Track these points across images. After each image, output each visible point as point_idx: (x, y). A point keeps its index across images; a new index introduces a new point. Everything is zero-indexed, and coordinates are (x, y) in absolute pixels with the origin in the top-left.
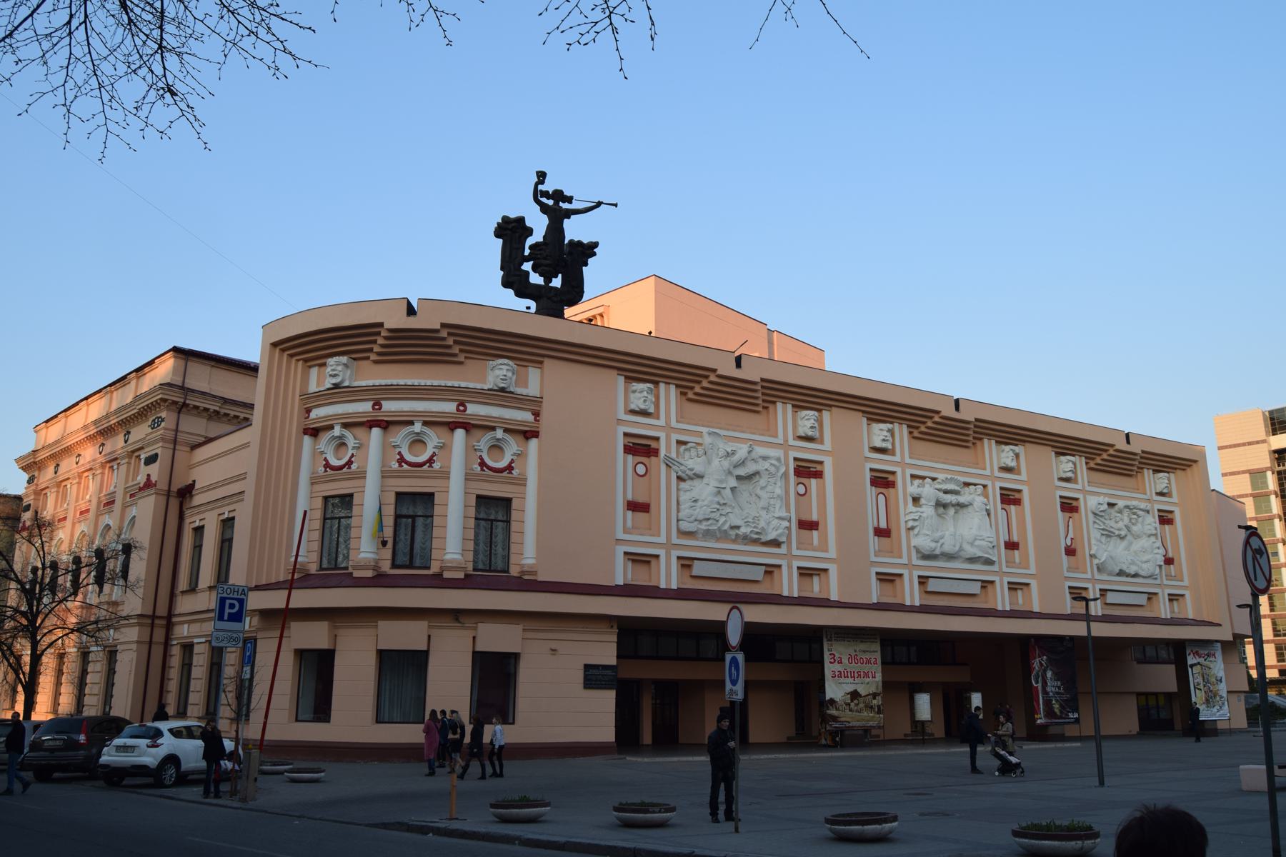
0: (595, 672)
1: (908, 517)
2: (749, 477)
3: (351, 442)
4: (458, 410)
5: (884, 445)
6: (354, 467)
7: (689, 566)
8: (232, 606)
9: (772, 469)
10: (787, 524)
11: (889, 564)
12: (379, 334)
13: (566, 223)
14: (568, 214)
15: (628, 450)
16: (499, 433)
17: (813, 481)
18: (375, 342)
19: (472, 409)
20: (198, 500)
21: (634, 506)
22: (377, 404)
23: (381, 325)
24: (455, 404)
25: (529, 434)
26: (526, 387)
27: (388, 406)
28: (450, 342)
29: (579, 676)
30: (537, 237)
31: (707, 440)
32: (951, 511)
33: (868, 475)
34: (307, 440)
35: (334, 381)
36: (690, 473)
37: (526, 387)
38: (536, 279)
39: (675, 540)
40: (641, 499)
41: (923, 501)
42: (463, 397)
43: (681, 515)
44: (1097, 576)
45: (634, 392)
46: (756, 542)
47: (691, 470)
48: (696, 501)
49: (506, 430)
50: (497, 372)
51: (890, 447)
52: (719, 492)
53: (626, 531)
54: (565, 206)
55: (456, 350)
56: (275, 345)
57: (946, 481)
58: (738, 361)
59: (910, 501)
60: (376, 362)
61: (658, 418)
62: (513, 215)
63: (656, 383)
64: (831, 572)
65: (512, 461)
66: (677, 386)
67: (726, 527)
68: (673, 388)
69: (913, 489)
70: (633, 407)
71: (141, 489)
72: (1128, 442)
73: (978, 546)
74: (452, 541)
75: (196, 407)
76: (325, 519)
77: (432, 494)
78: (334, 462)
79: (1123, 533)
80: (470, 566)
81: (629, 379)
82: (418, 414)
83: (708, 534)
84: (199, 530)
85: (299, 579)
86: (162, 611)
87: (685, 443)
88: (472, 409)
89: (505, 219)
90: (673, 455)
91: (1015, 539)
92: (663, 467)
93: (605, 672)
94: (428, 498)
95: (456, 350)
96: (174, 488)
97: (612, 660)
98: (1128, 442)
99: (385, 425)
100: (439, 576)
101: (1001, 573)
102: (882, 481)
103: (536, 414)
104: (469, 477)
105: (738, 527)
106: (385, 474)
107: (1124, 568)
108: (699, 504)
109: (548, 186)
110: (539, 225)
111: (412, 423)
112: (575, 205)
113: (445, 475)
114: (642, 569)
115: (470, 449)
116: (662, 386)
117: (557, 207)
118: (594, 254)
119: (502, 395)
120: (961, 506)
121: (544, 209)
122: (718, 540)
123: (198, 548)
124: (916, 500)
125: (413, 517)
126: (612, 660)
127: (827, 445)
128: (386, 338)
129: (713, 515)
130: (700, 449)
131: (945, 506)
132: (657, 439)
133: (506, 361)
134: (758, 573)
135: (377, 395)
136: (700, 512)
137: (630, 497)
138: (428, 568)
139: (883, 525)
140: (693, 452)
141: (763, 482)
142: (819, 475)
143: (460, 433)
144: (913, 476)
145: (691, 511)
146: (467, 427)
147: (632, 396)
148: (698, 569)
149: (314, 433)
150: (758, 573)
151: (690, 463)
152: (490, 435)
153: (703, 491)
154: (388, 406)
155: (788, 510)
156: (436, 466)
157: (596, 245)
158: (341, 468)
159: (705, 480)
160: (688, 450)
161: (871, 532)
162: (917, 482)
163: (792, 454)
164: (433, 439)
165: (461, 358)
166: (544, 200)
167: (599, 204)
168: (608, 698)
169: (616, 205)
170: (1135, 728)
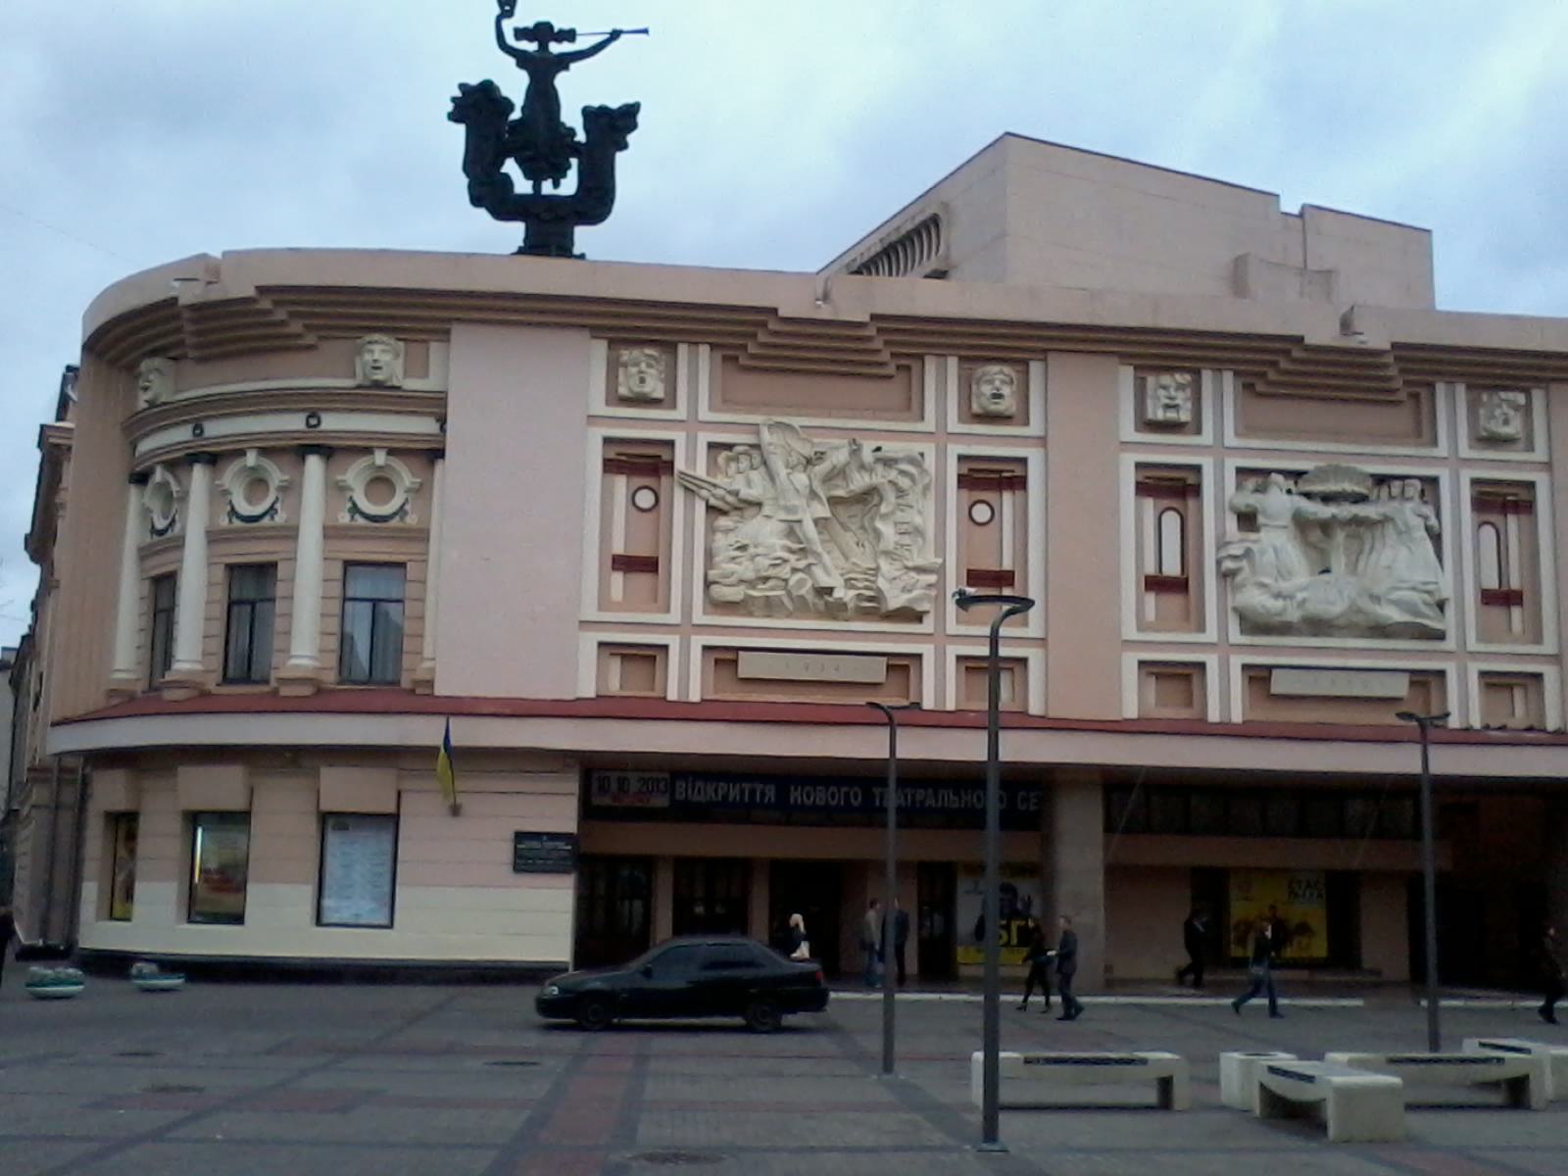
0: (535, 844)
1: (1223, 553)
2: (867, 497)
3: (174, 487)
4: (308, 424)
5: (1171, 415)
7: (735, 662)
9: (904, 482)
10: (932, 578)
11: (1174, 646)
12: (177, 317)
13: (562, 81)
14: (564, 61)
15: (611, 466)
16: (380, 458)
17: (1007, 496)
18: (179, 330)
19: (331, 422)
21: (626, 564)
22: (198, 429)
23: (175, 300)
24: (303, 417)
25: (436, 454)
26: (425, 375)
27: (215, 429)
28: (281, 315)
29: (506, 852)
30: (516, 115)
31: (767, 437)
32: (1340, 536)
33: (1128, 479)
34: (133, 491)
35: (148, 396)
36: (730, 499)
37: (425, 375)
38: (522, 186)
39: (699, 617)
40: (642, 551)
41: (1261, 519)
42: (314, 403)
43: (713, 574)
45: (625, 365)
46: (866, 614)
47: (736, 494)
48: (743, 548)
49: (391, 452)
50: (368, 357)
52: (791, 533)
53: (604, 603)
54: (555, 48)
55: (296, 327)
57: (1322, 474)
59: (1231, 523)
60: (203, 360)
61: (673, 406)
62: (474, 81)
63: (670, 348)
64: (1031, 664)
65: (406, 501)
66: (713, 346)
67: (806, 590)
68: (704, 351)
69: (1248, 499)
70: (623, 391)
73: (1397, 603)
74: (303, 643)
77: (274, 565)
80: (330, 677)
81: (613, 343)
83: (770, 606)
85: (125, 704)
87: (729, 447)
88: (331, 422)
89: (462, 87)
90: (701, 471)
91: (1515, 584)
92: (679, 495)
93: (550, 844)
94: (265, 571)
95: (296, 327)
97: (570, 826)
99: (214, 460)
100: (275, 693)
101: (1466, 654)
102: (1171, 487)
103: (442, 421)
104: (331, 533)
105: (830, 591)
106: (214, 537)
108: (752, 550)
109: (525, 16)
110: (514, 85)
111: (242, 453)
112: (582, 44)
113: (291, 533)
114: (638, 670)
115: (336, 489)
116: (683, 350)
117: (544, 54)
118: (633, 126)
119: (378, 395)
120: (1357, 521)
121: (523, 59)
122: (790, 615)
124: (1248, 520)
125: (253, 604)
126: (570, 826)
127: (1035, 428)
128: (194, 321)
129: (771, 572)
130: (755, 454)
131: (1326, 526)
132: (670, 444)
133: (376, 337)
134: (877, 671)
135: (197, 411)
136: (745, 569)
137: (619, 548)
138: (266, 682)
139: (1172, 568)
140: (744, 463)
141: (884, 509)
142: (1019, 483)
143: (314, 464)
144: (1241, 472)
145: (732, 566)
146: (327, 452)
147: (621, 371)
148: (748, 666)
149: (141, 478)
150: (877, 671)
151: (738, 484)
152: (363, 462)
153: (765, 532)
154: (215, 429)
155: (940, 550)
156: (280, 518)
158: (161, 533)
159: (766, 510)
160: (736, 459)
162: (1251, 483)
163: (955, 450)
164: (276, 475)
167: (615, 35)
169: (645, 31)
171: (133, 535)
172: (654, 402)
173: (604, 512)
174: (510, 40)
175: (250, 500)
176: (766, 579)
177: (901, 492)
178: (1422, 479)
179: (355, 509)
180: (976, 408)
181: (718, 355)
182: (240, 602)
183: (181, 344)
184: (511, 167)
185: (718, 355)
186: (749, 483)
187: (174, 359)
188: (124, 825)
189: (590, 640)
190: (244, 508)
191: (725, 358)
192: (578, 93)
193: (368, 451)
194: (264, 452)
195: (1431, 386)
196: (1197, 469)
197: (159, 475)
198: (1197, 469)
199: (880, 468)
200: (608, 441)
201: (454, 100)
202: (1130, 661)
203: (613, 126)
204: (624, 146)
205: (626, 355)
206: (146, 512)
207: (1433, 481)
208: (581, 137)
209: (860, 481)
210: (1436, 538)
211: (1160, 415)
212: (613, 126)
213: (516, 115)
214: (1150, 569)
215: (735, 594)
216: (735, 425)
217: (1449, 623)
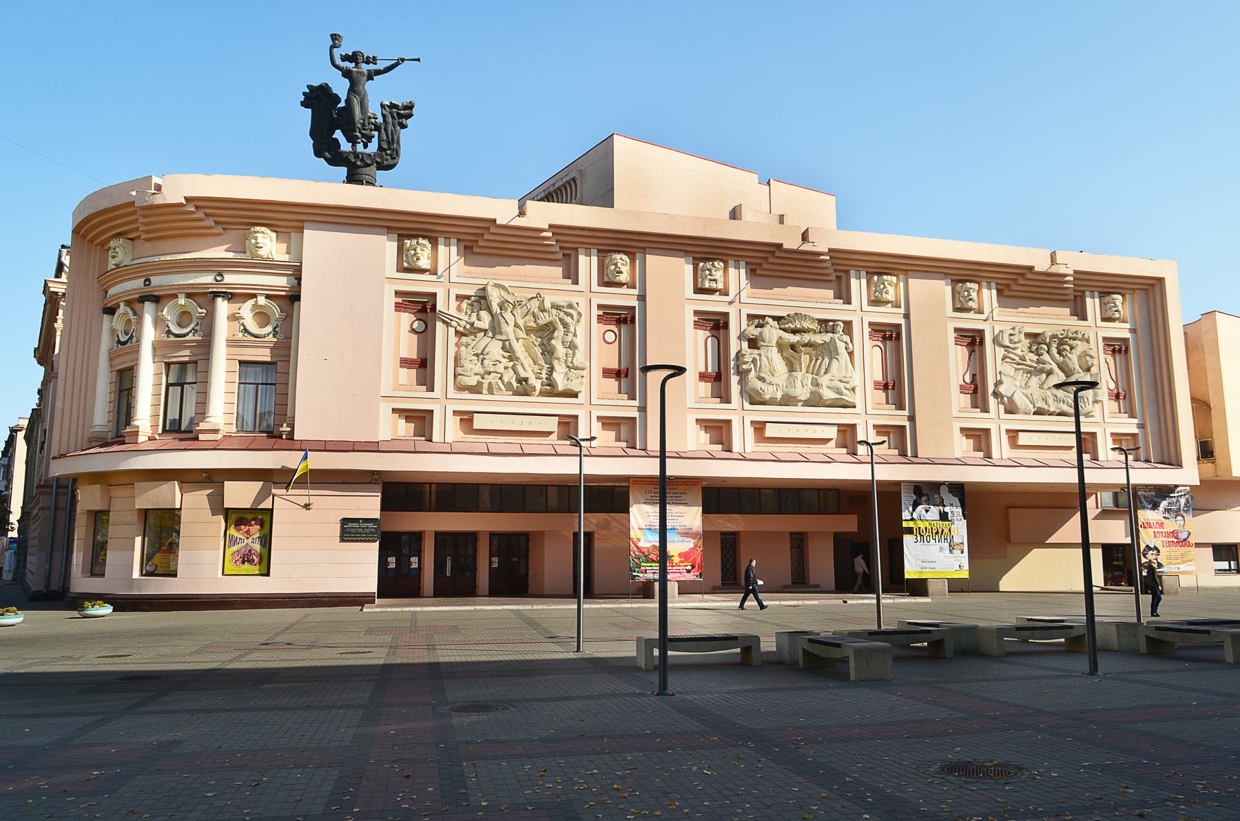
0: (356, 525)
7: (471, 420)
9: (568, 319)
15: (399, 307)
19: (229, 278)
30: (342, 104)
38: (345, 146)
42: (218, 267)
43: (459, 370)
47: (472, 324)
49: (268, 297)
51: (720, 286)
55: (210, 222)
59: (745, 344)
60: (147, 240)
69: (753, 331)
79: (1047, 367)
81: (401, 238)
82: (180, 287)
87: (468, 297)
88: (229, 278)
90: (453, 311)
93: (365, 525)
97: (376, 514)
99: (156, 300)
104: (231, 343)
105: (526, 380)
109: (346, 48)
112: (381, 65)
117: (357, 68)
120: (809, 345)
121: (347, 74)
124: (753, 343)
126: (376, 514)
149: (111, 311)
152: (252, 302)
157: (410, 107)
158: (125, 343)
163: (596, 301)
165: (219, 230)
166: (347, 64)
167: (403, 60)
168: (369, 552)
171: (106, 342)
174: (338, 62)
175: (180, 325)
176: (490, 373)
177: (565, 325)
178: (844, 322)
180: (606, 279)
181: (462, 245)
183: (137, 229)
184: (338, 134)
185: (462, 245)
187: (132, 239)
188: (99, 518)
190: (175, 329)
191: (465, 247)
192: (378, 94)
193: (254, 296)
194: (189, 296)
195: (847, 272)
196: (726, 315)
197: (122, 308)
198: (726, 315)
199: (554, 311)
200: (397, 293)
201: (304, 94)
203: (400, 114)
204: (404, 126)
206: (113, 331)
207: (848, 325)
208: (380, 120)
209: (544, 319)
210: (851, 354)
211: (707, 285)
212: (400, 114)
213: (342, 104)
214: (703, 370)
217: (857, 399)
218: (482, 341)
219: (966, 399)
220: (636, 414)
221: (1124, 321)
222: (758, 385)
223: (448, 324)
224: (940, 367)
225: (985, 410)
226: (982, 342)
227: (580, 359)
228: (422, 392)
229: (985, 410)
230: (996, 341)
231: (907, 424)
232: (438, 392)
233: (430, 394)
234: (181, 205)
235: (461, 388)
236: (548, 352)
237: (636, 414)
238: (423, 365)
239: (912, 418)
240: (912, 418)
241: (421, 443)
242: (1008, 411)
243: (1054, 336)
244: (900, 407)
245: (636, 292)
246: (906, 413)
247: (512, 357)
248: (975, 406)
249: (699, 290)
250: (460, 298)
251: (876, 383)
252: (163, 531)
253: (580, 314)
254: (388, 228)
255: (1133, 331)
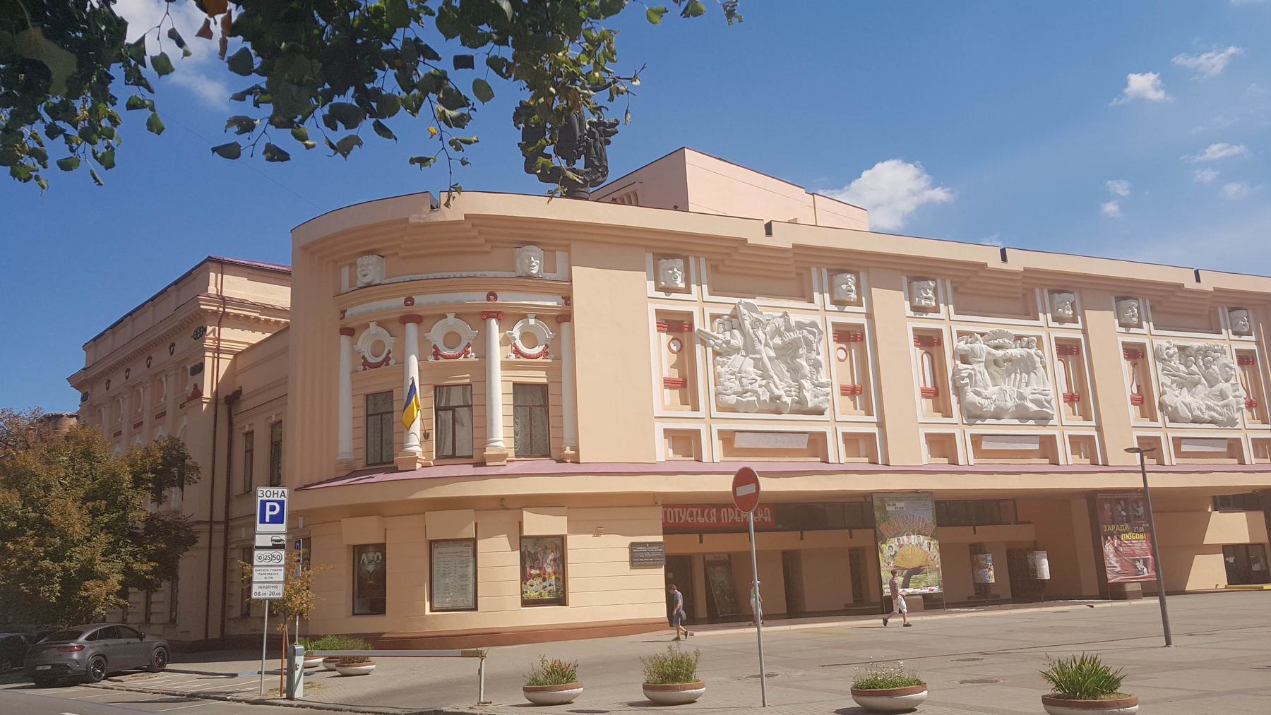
4: (488, 299)
6: (392, 362)
8: (273, 508)
9: (811, 337)
16: (532, 321)
20: (245, 405)
25: (565, 317)
28: (475, 233)
34: (345, 340)
38: (558, 162)
39: (715, 414)
44: (1169, 424)
47: (728, 343)
56: (304, 248)
57: (997, 335)
58: (768, 229)
60: (404, 258)
67: (766, 397)
71: (189, 399)
72: (1198, 280)
75: (237, 316)
76: (368, 416)
78: (371, 360)
83: (748, 407)
84: (249, 435)
86: (219, 515)
87: (719, 316)
90: (708, 330)
93: (651, 549)
96: (221, 397)
98: (1198, 280)
99: (418, 319)
103: (568, 300)
105: (779, 398)
107: (1198, 413)
116: (692, 260)
119: (528, 282)
123: (250, 451)
131: (996, 362)
144: (960, 334)
149: (349, 332)
161: (918, 394)
168: (657, 577)
170: (1223, 582)
172: (678, 291)
173: (660, 353)
179: (517, 352)
182: (446, 409)
186: (733, 336)
189: (659, 427)
193: (525, 316)
196: (939, 332)
198: (939, 332)
202: (923, 431)
204: (609, 143)
205: (664, 263)
207: (1039, 338)
210: (1045, 367)
212: (606, 131)
215: (732, 399)
216: (724, 305)
218: (737, 360)
219: (1134, 411)
220: (875, 430)
221: (1249, 334)
222: (977, 399)
223: (704, 343)
224: (1114, 379)
225: (1154, 419)
226: (1144, 355)
227: (823, 379)
228: (687, 412)
229: (1154, 419)
230: (1157, 357)
231: (1095, 434)
232: (702, 413)
233: (695, 414)
234: (459, 222)
235: (721, 408)
236: (796, 372)
237: (875, 430)
238: (684, 384)
239: (1099, 428)
240: (1099, 428)
241: (689, 464)
242: (1171, 421)
243: (1199, 349)
244: (1087, 418)
245: (863, 309)
246: (1093, 423)
247: (765, 375)
248: (1143, 416)
249: (915, 309)
250: (714, 317)
251: (1065, 396)
252: (544, 563)
253: (821, 332)
254: (646, 247)
255: (1258, 343)
